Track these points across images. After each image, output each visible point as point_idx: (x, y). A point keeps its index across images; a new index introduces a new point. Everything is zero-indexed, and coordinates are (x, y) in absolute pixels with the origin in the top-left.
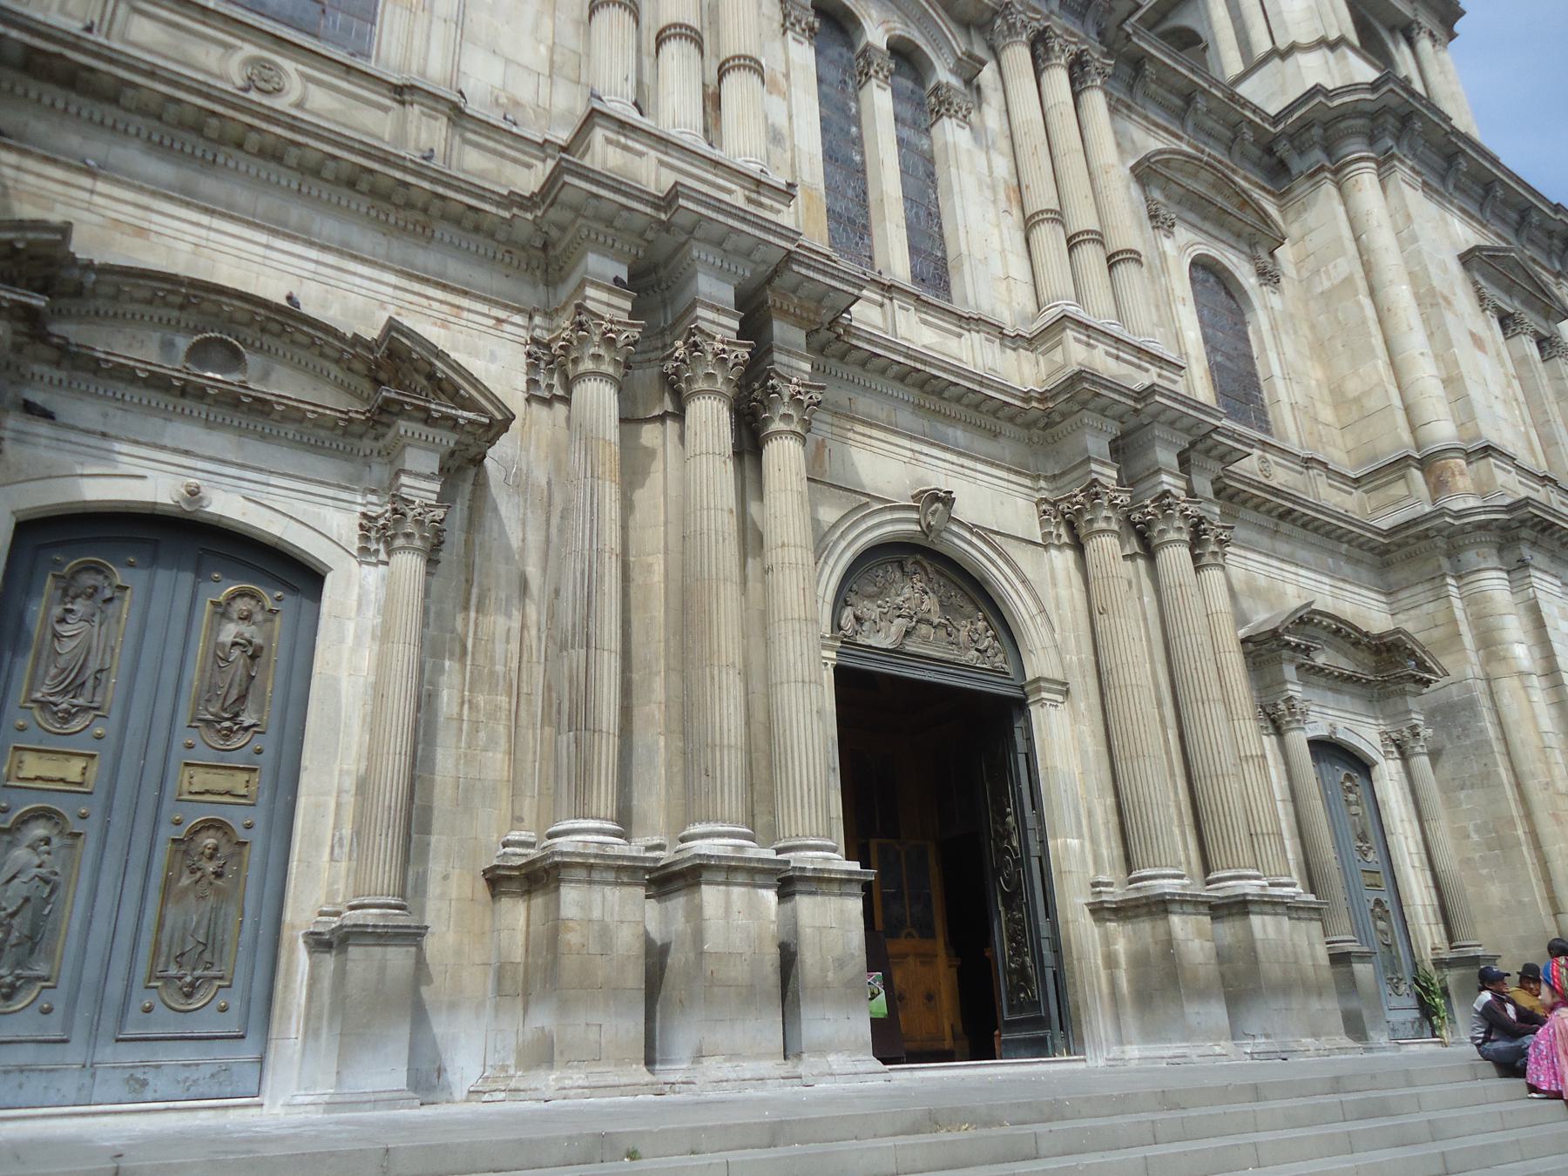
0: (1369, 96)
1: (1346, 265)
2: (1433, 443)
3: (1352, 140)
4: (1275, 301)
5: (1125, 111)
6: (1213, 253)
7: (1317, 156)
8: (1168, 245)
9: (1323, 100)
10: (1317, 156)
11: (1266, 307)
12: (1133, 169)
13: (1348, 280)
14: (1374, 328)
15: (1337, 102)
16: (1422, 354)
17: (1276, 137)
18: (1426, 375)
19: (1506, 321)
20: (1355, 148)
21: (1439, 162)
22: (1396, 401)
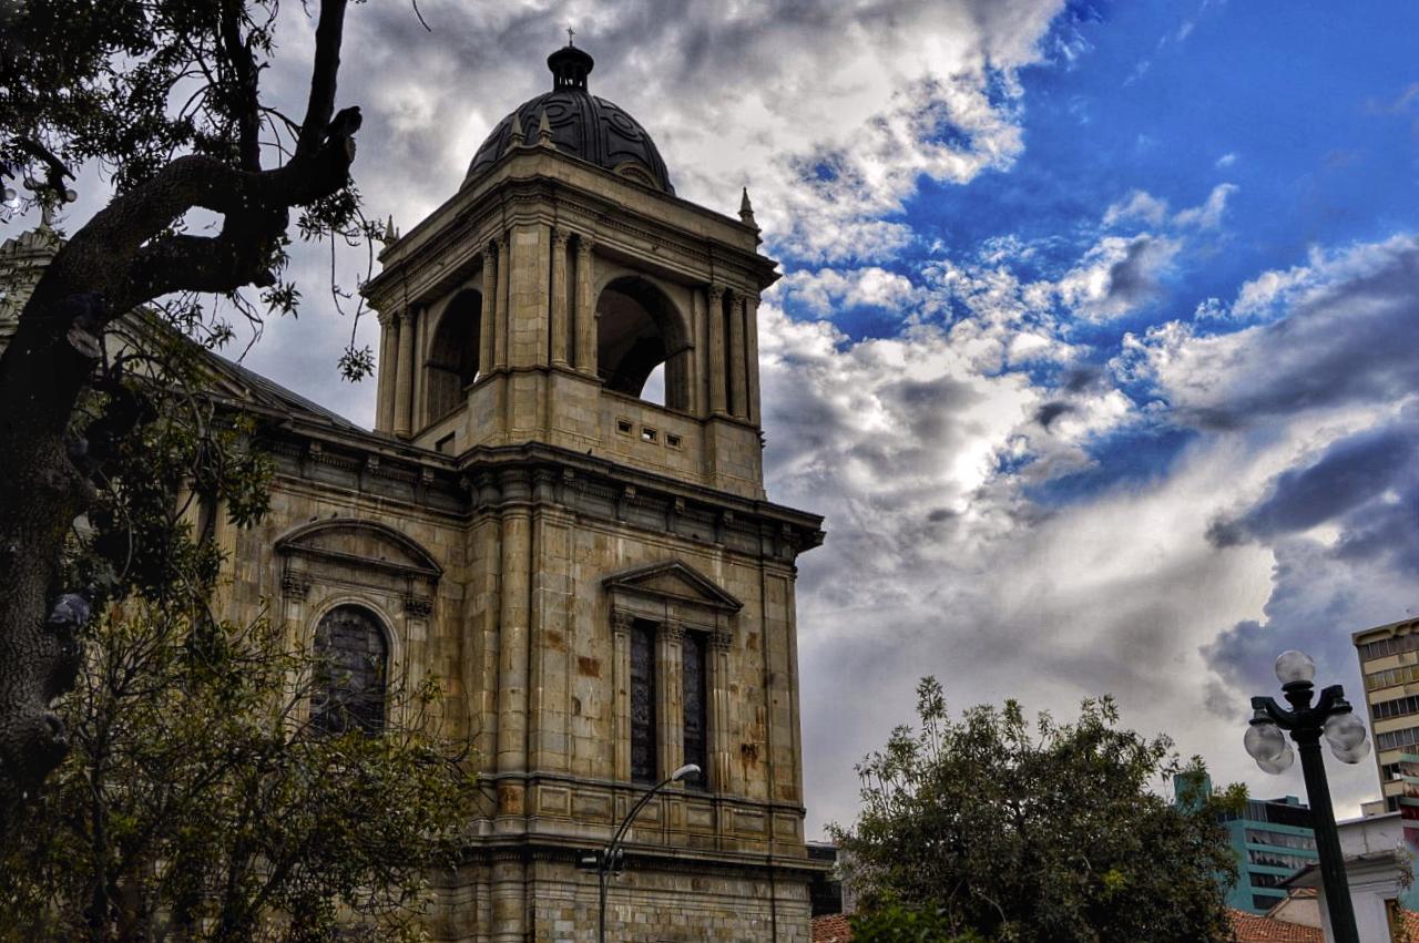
0: (519, 457)
1: (483, 602)
2: (502, 769)
3: (511, 486)
4: (418, 633)
5: (287, 486)
6: (356, 600)
7: (489, 494)
8: (295, 612)
9: (482, 458)
10: (489, 494)
11: (405, 640)
12: (277, 544)
13: (483, 613)
14: (488, 661)
15: (496, 459)
16: (513, 691)
17: (458, 475)
18: (515, 704)
19: (647, 634)
20: (515, 492)
21: (610, 492)
22: (488, 727)
